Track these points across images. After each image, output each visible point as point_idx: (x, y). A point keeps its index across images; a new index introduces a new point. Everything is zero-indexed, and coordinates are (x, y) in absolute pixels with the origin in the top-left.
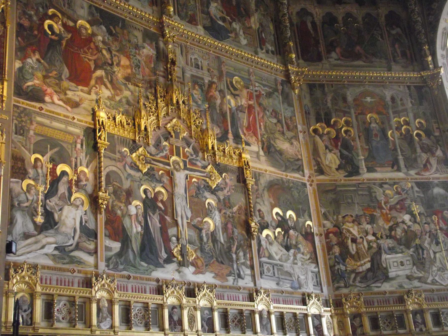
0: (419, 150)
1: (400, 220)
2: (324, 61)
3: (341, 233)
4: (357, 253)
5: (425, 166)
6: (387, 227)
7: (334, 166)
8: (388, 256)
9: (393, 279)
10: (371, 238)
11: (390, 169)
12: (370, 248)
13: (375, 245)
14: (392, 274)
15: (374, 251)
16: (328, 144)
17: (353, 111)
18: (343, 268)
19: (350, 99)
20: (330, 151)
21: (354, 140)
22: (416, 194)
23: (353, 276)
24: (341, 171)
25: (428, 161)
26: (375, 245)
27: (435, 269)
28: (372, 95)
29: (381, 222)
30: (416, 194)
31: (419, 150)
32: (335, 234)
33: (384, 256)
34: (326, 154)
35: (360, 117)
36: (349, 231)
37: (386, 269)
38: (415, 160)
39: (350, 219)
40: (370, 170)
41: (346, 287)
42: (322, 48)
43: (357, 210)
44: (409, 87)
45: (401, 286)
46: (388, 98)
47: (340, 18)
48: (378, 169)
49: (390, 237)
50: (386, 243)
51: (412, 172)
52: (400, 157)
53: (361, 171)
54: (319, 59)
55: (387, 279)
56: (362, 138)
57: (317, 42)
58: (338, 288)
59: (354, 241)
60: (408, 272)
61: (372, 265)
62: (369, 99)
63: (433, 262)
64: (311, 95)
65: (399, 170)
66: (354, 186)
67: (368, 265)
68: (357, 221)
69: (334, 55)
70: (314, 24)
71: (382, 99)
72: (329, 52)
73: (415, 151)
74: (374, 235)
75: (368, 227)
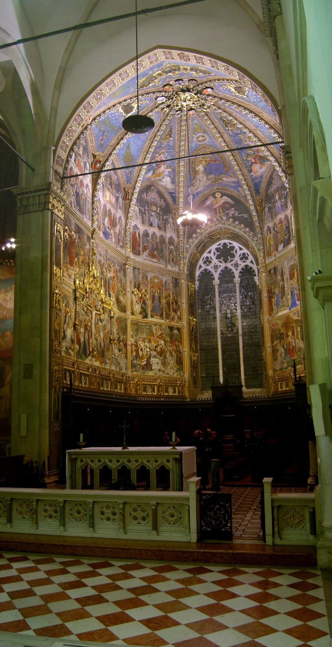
0: (171, 310)
1: (160, 343)
2: (141, 256)
3: (137, 345)
4: (142, 356)
5: (173, 318)
6: (155, 346)
7: (138, 312)
8: (153, 359)
9: (153, 370)
10: (148, 350)
11: (159, 317)
12: (147, 354)
13: (149, 354)
14: (153, 368)
15: (148, 356)
16: (137, 300)
17: (149, 285)
18: (136, 362)
19: (149, 278)
20: (138, 304)
21: (148, 300)
22: (168, 332)
23: (139, 366)
24: (141, 315)
25: (174, 316)
26: (149, 354)
27: (169, 367)
28: (158, 278)
29: (153, 343)
30: (168, 332)
31: (171, 310)
32: (135, 345)
33: (152, 359)
34: (136, 305)
35: (152, 288)
36: (140, 345)
37: (151, 365)
38: (169, 315)
39: (141, 339)
40: (152, 316)
41: (136, 371)
42: (141, 249)
43: (144, 336)
44: (173, 278)
45: (156, 374)
46: (164, 282)
47: (150, 235)
48: (155, 317)
49: (155, 350)
50: (154, 353)
51: (168, 321)
52: (164, 313)
53: (148, 317)
54: (139, 254)
55: (151, 369)
56: (151, 300)
57: (139, 245)
58: (133, 371)
59: (141, 350)
60: (159, 368)
61: (147, 362)
62: (156, 280)
63: (169, 364)
64: (134, 272)
65: (163, 319)
66: (145, 323)
67: (145, 362)
68: (144, 341)
69: (145, 253)
70: (139, 234)
71: (161, 281)
72: (143, 251)
73: (170, 311)
74: (149, 348)
75: (148, 344)
